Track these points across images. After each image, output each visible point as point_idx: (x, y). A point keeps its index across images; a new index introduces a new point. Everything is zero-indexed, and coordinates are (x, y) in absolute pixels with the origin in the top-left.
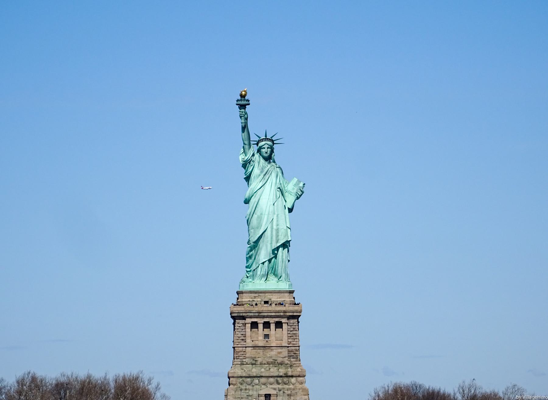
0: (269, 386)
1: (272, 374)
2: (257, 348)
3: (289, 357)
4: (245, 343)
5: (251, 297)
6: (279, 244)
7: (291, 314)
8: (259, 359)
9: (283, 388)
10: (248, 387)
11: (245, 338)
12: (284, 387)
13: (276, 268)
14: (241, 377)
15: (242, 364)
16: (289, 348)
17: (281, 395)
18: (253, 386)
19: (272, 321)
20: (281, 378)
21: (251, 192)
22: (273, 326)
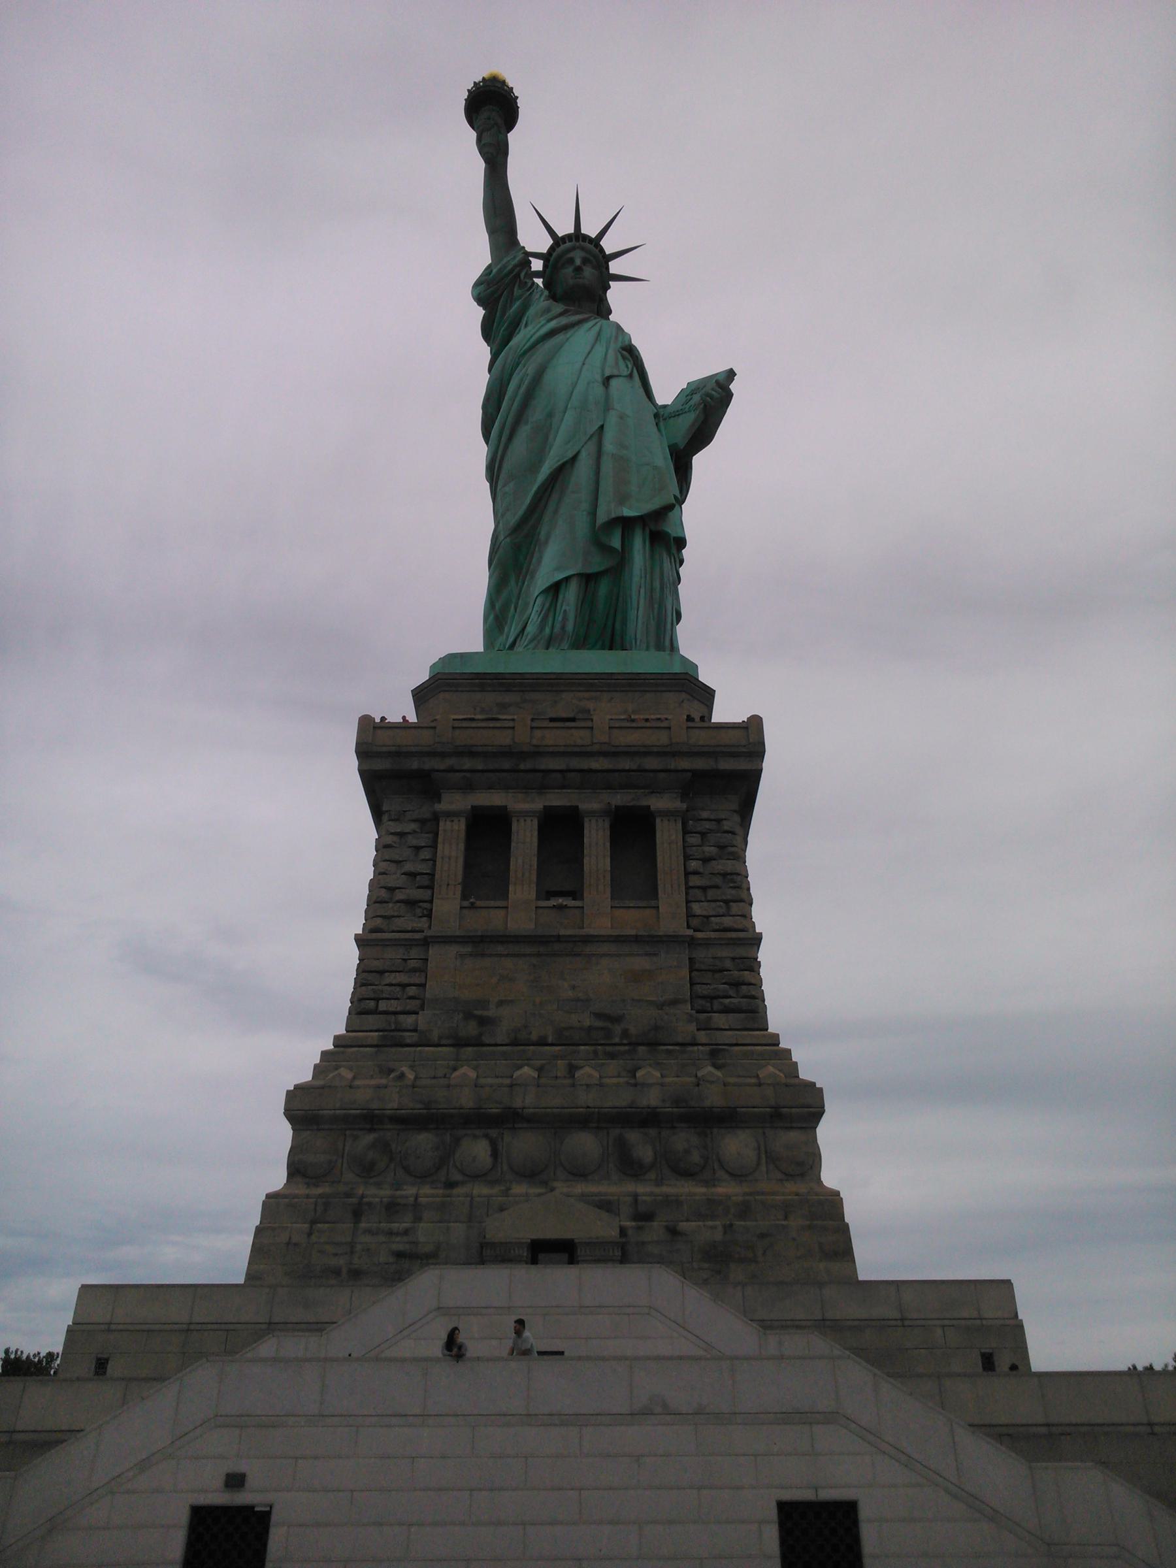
0: (561, 1187)
1: (586, 1099)
2: (500, 949)
4: (423, 923)
6: (627, 512)
7: (700, 764)
10: (410, 1191)
11: (429, 892)
12: (665, 1189)
13: (618, 626)
14: (371, 1120)
15: (391, 1040)
16: (700, 954)
18: (450, 1185)
19: (590, 803)
20: (653, 1132)
21: (509, 361)
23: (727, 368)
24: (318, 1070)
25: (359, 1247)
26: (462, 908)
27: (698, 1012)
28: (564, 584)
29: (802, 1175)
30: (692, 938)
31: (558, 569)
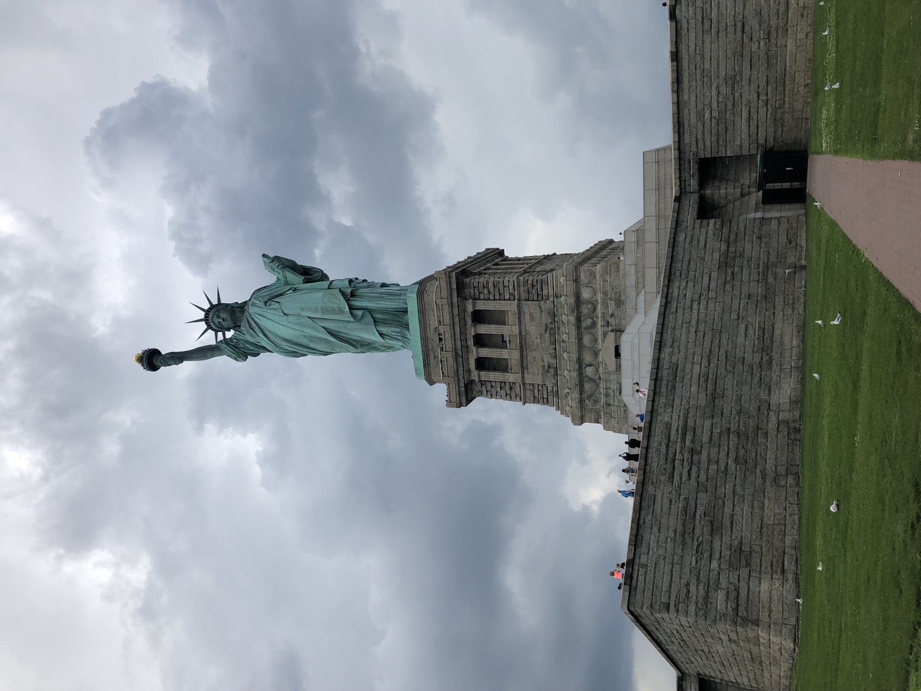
1: (573, 339)
2: (525, 361)
3: (539, 298)
4: (517, 385)
5: (435, 364)
6: (347, 309)
8: (545, 360)
9: (603, 317)
10: (602, 389)
12: (600, 316)
14: (581, 401)
16: (524, 296)
17: (617, 321)
18: (600, 378)
19: (471, 331)
22: (484, 329)
23: (261, 257)
24: (567, 416)
25: (618, 405)
26: (512, 373)
27: (543, 299)
28: (380, 332)
29: (594, 273)
30: (518, 299)
31: (374, 335)
